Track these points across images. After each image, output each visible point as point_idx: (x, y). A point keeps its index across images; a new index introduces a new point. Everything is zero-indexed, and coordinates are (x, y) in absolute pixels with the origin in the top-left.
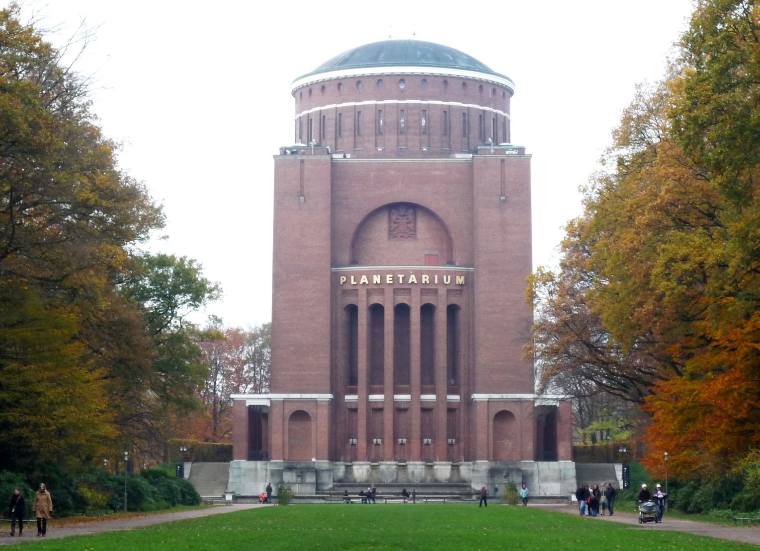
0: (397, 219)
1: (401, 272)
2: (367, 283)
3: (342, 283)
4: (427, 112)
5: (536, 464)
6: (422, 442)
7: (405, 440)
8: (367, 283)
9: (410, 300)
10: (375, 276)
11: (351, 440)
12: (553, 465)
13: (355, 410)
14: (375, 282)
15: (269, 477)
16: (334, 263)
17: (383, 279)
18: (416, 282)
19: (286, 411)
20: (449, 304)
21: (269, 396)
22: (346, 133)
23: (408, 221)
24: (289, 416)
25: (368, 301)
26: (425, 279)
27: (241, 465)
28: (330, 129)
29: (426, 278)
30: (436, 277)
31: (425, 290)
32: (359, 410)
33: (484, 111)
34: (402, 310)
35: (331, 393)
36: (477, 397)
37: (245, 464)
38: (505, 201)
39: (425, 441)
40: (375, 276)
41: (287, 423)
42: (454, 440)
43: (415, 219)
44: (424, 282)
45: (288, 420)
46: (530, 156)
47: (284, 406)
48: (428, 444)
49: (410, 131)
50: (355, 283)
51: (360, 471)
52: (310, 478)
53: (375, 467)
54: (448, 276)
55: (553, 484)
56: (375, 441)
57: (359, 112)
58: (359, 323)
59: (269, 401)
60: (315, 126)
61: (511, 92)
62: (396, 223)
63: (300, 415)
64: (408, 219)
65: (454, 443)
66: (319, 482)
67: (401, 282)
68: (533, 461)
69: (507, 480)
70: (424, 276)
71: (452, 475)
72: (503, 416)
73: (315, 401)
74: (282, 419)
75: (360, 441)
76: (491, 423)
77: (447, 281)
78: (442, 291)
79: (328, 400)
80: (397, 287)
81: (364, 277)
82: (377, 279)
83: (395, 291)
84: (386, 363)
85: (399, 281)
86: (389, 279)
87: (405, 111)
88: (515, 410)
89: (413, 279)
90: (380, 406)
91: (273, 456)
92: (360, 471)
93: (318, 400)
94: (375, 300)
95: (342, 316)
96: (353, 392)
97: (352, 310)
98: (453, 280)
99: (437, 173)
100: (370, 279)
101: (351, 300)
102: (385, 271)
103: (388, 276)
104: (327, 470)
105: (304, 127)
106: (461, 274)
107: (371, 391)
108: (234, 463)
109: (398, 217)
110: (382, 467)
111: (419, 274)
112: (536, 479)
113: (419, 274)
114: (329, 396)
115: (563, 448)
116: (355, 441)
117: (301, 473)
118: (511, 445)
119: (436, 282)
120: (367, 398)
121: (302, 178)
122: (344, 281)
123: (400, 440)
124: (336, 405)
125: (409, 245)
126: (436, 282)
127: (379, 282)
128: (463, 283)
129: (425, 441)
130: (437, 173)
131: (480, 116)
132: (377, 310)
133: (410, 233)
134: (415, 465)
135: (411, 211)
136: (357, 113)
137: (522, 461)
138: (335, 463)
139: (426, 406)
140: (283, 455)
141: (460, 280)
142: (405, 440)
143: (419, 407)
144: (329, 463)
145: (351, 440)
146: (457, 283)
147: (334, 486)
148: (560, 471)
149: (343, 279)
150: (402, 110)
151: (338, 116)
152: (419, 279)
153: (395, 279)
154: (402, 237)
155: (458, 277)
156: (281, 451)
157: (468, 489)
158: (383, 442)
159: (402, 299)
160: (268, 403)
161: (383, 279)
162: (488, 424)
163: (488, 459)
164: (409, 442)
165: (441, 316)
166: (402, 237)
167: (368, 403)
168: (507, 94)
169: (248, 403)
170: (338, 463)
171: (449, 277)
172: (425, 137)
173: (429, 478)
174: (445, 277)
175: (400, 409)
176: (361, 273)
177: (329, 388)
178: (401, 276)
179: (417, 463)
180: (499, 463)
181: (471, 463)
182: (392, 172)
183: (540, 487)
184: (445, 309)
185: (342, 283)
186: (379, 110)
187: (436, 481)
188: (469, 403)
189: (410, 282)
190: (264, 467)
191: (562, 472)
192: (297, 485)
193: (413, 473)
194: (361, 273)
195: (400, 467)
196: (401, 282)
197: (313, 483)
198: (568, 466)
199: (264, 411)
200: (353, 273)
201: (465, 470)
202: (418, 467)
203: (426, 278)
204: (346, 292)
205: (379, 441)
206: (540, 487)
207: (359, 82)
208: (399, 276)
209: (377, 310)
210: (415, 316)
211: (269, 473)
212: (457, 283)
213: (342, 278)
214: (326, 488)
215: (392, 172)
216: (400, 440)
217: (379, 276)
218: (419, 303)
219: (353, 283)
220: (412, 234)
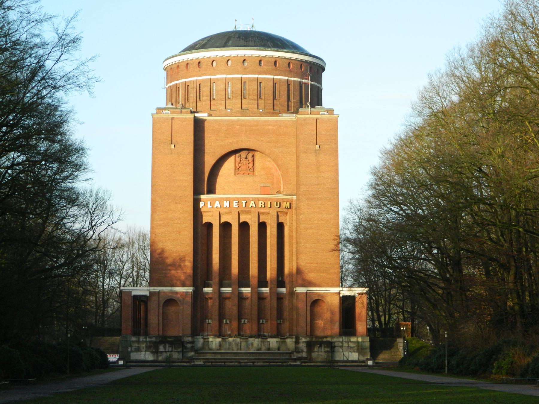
1: (244, 199)
6: (259, 322)
8: (219, 206)
11: (207, 320)
14: (225, 206)
19: (161, 299)
22: (205, 98)
28: (192, 95)
34: (244, 227)
35: (193, 286)
36: (300, 290)
39: (261, 321)
40: (225, 202)
41: (161, 308)
46: (338, 115)
59: (148, 292)
60: (182, 92)
61: (323, 69)
67: (244, 206)
81: (217, 203)
84: (232, 265)
86: (235, 204)
89: (252, 204)
96: (208, 286)
97: (209, 225)
99: (270, 127)
102: (232, 198)
105: (173, 94)
107: (221, 285)
111: (256, 201)
120: (219, 290)
123: (243, 321)
124: (197, 295)
125: (249, 179)
130: (270, 127)
132: (226, 227)
135: (250, 155)
143: (257, 296)
145: (207, 320)
149: (202, 204)
160: (147, 293)
168: (320, 70)
169: (133, 293)
170: (198, 337)
176: (215, 200)
178: (244, 202)
182: (237, 127)
185: (201, 207)
188: (292, 293)
213: (201, 203)
215: (237, 127)
217: (228, 202)
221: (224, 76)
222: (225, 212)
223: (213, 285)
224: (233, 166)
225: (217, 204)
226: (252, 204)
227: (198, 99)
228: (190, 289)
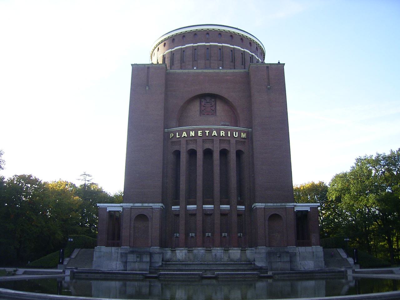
0: (205, 105)
2: (186, 136)
3: (171, 138)
4: (222, 50)
5: (297, 248)
7: (210, 234)
8: (186, 136)
9: (213, 147)
10: (191, 132)
11: (175, 234)
12: (309, 249)
13: (178, 215)
14: (191, 136)
15: (119, 257)
16: (166, 126)
17: (196, 134)
18: (216, 135)
20: (237, 149)
21: (121, 204)
23: (211, 106)
25: (187, 148)
26: (222, 133)
27: (102, 250)
29: (223, 133)
30: (229, 132)
31: (222, 140)
32: (180, 215)
33: (252, 55)
34: (208, 153)
35: (162, 203)
37: (104, 249)
38: (269, 89)
39: (223, 234)
40: (191, 132)
43: (215, 104)
44: (221, 135)
46: (284, 64)
48: (225, 237)
49: (212, 58)
50: (179, 137)
51: (181, 254)
52: (146, 259)
54: (237, 133)
55: (309, 262)
56: (191, 234)
57: (184, 51)
58: (181, 160)
59: (122, 208)
62: (204, 106)
63: (142, 217)
64: (211, 104)
65: (241, 236)
66: (152, 261)
67: (207, 135)
68: (295, 247)
69: (280, 259)
70: (221, 132)
71: (241, 256)
72: (274, 217)
76: (267, 222)
77: (236, 135)
78: (233, 141)
80: (205, 138)
81: (184, 133)
82: (192, 134)
83: (204, 141)
85: (206, 135)
87: (209, 49)
89: (215, 133)
92: (181, 254)
93: (153, 207)
94: (191, 146)
95: (171, 157)
97: (177, 154)
98: (240, 135)
99: (228, 77)
100: (188, 134)
101: (176, 148)
102: (197, 129)
103: (199, 132)
104: (158, 253)
106: (244, 132)
108: (97, 248)
109: (206, 103)
110: (195, 251)
112: (298, 258)
113: (218, 131)
115: (314, 237)
116: (178, 235)
117: (140, 255)
118: (279, 237)
119: (229, 136)
121: (148, 77)
122: (172, 136)
123: (207, 234)
124: (165, 212)
125: (212, 119)
126: (229, 136)
127: (193, 135)
128: (246, 137)
129: (223, 234)
130: (228, 77)
131: (251, 58)
132: (192, 153)
133: (212, 112)
134: (218, 250)
135: (213, 100)
136: (182, 52)
137: (288, 247)
138: (164, 249)
141: (243, 135)
142: (210, 234)
144: (160, 249)
146: (242, 137)
148: (313, 253)
149: (172, 135)
150: (208, 49)
151: (172, 55)
152: (219, 133)
153: (203, 133)
154: (208, 114)
155: (242, 134)
157: (253, 266)
158: (196, 235)
159: (208, 146)
161: (196, 134)
165: (233, 156)
166: (208, 114)
170: (167, 249)
171: (237, 133)
172: (221, 62)
173: (226, 258)
174: (234, 133)
175: (207, 214)
178: (207, 132)
179: (218, 248)
180: (273, 248)
181: (253, 249)
183: (300, 263)
184: (235, 152)
185: (171, 138)
186: (195, 49)
187: (232, 260)
188: (250, 210)
189: (213, 135)
190: (117, 251)
191: (315, 254)
192: (137, 263)
193: (216, 255)
194: (182, 131)
195: (207, 251)
196: (207, 135)
197: (148, 262)
198: (319, 250)
199: (117, 215)
200: (178, 131)
201: (249, 253)
202: (219, 251)
203: (223, 133)
204: (173, 143)
205: (193, 234)
206: (300, 263)
207: (184, 36)
208: (206, 131)
209: (192, 153)
210: (216, 156)
211: (119, 255)
212: (242, 137)
214: (157, 265)
216: (207, 234)
217: (194, 132)
218: (219, 148)
219: (177, 137)
220: (214, 112)
221: (192, 45)
222: (191, 140)
224: (198, 108)
225: (185, 134)
226: (215, 133)
227: (172, 65)
228: (159, 205)
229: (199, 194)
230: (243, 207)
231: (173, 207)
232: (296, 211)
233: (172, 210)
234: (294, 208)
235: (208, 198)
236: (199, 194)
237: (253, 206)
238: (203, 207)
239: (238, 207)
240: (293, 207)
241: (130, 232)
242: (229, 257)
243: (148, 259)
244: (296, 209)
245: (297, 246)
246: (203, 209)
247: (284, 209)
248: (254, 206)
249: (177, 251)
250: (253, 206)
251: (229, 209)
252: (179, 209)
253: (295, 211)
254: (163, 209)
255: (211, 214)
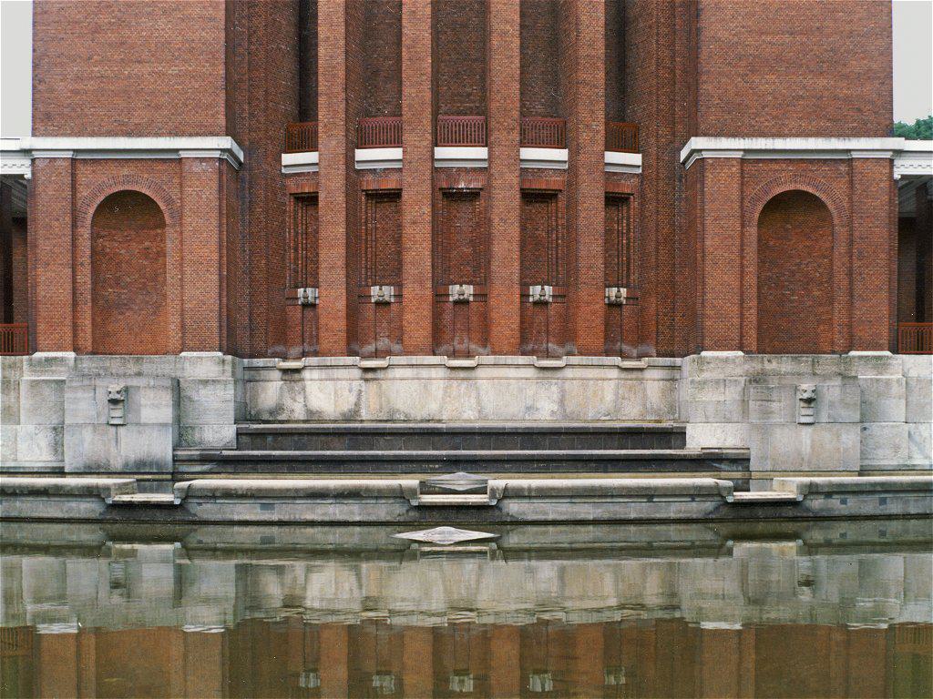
13: (310, 200)
19: (83, 192)
24: (92, 211)
32: (322, 196)
35: (230, 131)
42: (624, 291)
45: (89, 221)
47: (73, 175)
48: (541, 304)
53: (370, 375)
56: (375, 291)
59: (28, 162)
63: (129, 210)
68: (888, 353)
73: (174, 160)
74: (68, 219)
75: (329, 294)
76: (753, 231)
79: (217, 154)
88: (832, 193)
90: (391, 184)
91: (41, 340)
93: (183, 155)
114: (226, 142)
120: (350, 159)
129: (535, 291)
137: (853, 353)
139: (540, 185)
140: (75, 336)
142: (469, 290)
145: (301, 291)
147: (238, 434)
156: (68, 322)
158: (399, 296)
160: (22, 167)
162: (742, 234)
163: (741, 348)
164: (481, 296)
167: (353, 174)
177: (222, 120)
197: (165, 425)
205: (388, 292)
223: (322, 138)
229: (416, 90)
230: (636, 159)
231: (287, 159)
232: (904, 177)
233: (283, 171)
234: (891, 161)
235: (461, 111)
236: (416, 90)
237: (684, 154)
238: (437, 156)
239: (613, 157)
240: (888, 155)
241: (74, 281)
242: (562, 402)
243: (166, 414)
244: (903, 168)
245: (893, 352)
246: (437, 165)
247: (843, 168)
248: (693, 152)
249: (307, 374)
250: (684, 154)
251: (566, 166)
252: (315, 169)
253: (897, 176)
254: (236, 166)
255: (474, 195)
